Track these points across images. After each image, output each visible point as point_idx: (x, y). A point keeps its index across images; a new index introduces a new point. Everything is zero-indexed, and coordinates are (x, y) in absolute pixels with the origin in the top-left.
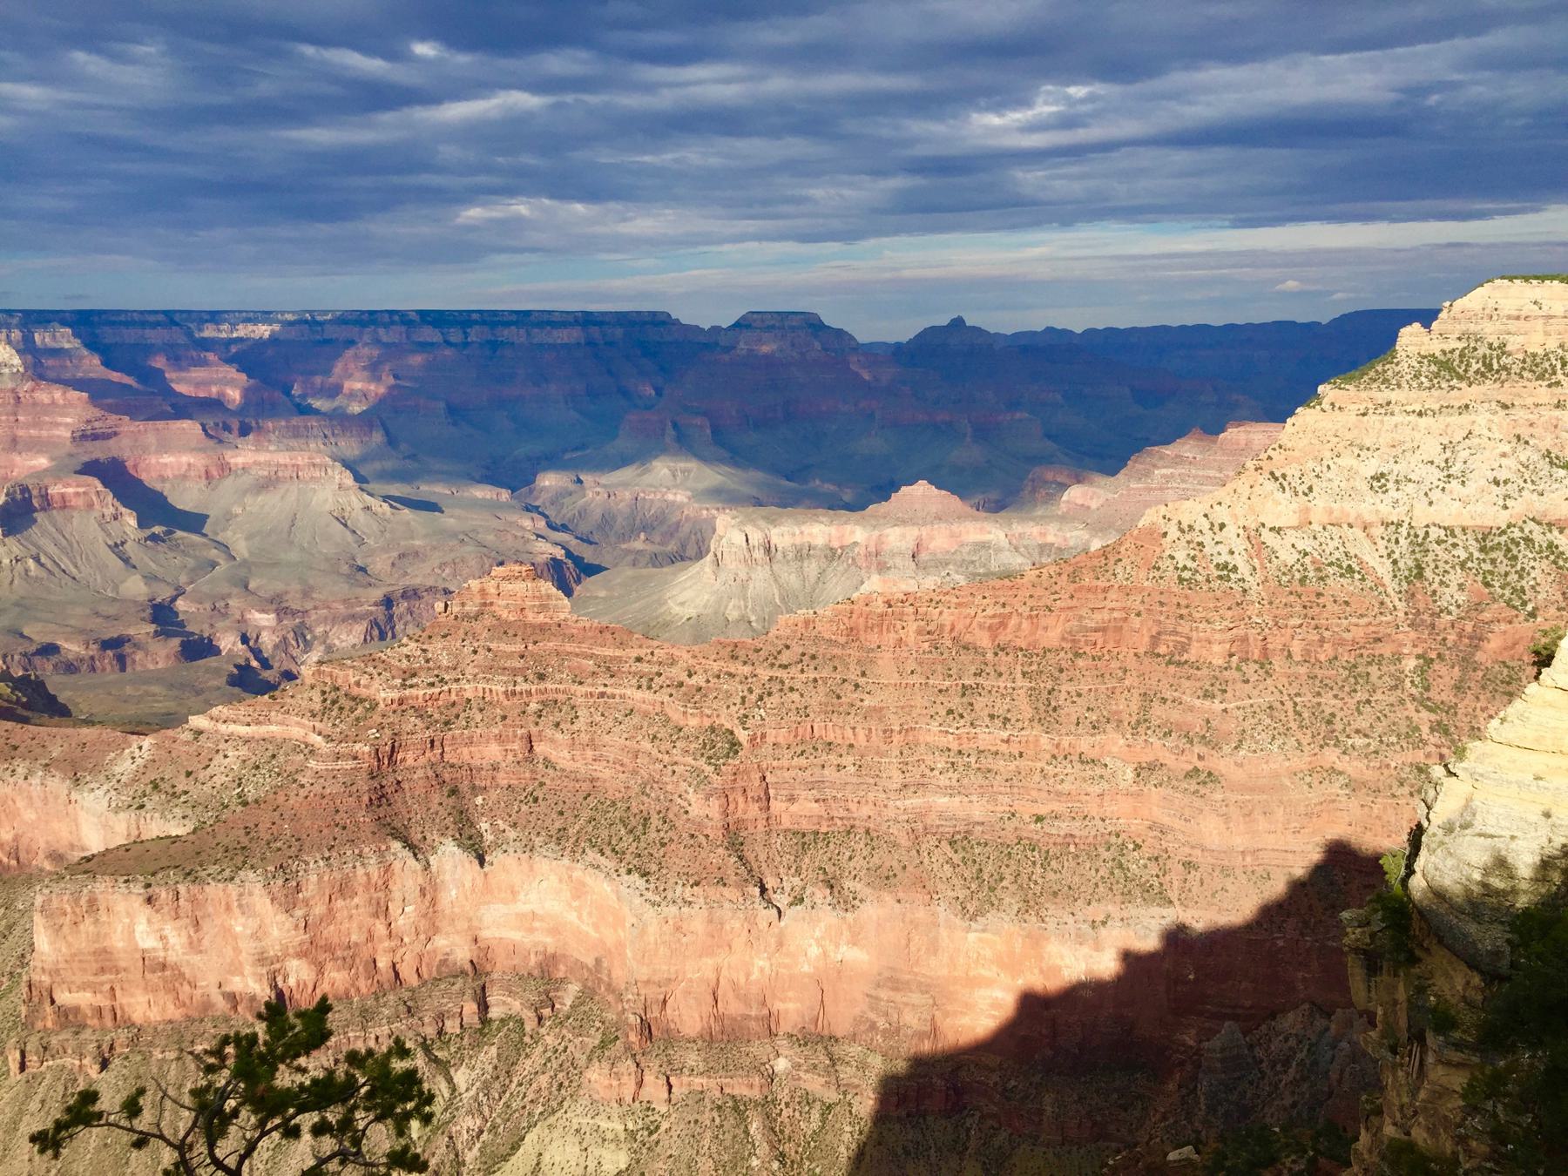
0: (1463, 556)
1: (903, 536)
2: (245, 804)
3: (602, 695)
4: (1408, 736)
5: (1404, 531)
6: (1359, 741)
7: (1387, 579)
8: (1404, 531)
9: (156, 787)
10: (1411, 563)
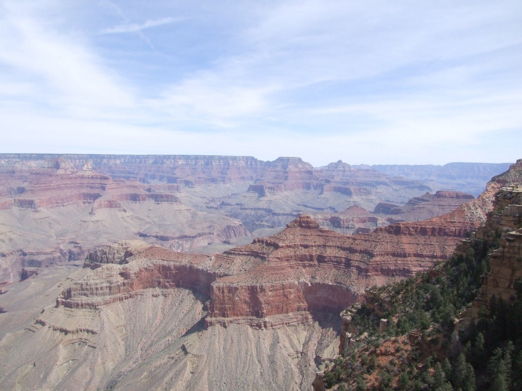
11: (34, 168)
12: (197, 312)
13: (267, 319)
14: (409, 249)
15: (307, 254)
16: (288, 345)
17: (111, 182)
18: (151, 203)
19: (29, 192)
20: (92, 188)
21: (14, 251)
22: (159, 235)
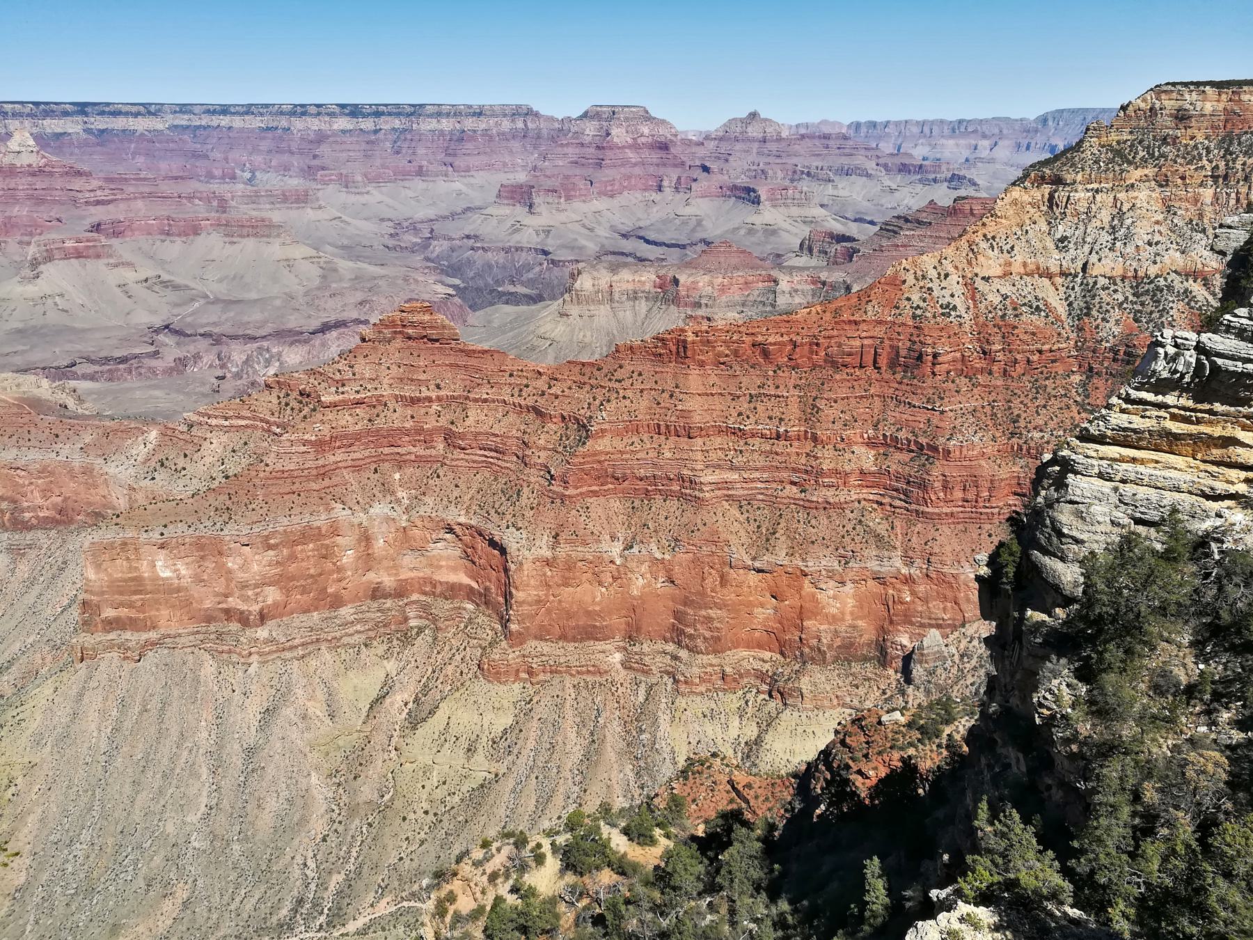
0: (1121, 299)
1: (711, 284)
2: (227, 477)
3: (485, 401)
4: (1071, 430)
5: (1078, 280)
6: (1037, 435)
7: (1064, 317)
8: (1078, 280)
9: (162, 465)
10: (1082, 304)
14: (699, 409)
20: (40, 201)
22: (216, 330)
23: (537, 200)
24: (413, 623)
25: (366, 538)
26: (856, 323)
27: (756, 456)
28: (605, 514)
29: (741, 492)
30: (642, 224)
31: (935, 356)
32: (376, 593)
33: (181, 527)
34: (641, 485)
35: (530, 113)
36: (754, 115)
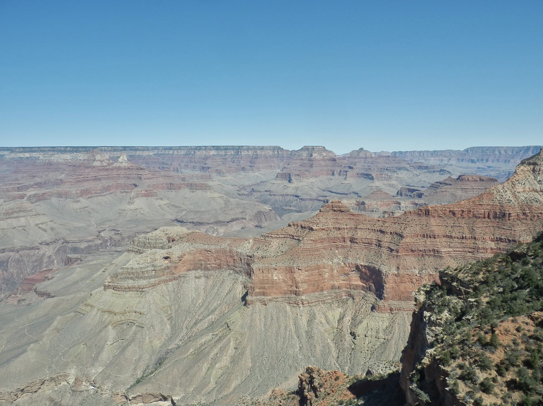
11: (70, 161)
12: (238, 291)
13: (303, 297)
14: (437, 230)
15: (339, 236)
16: (324, 321)
17: (147, 172)
18: (186, 192)
19: (68, 184)
21: (56, 240)
23: (293, 178)
24: (344, 297)
25: (332, 270)
26: (481, 205)
27: (457, 244)
28: (410, 261)
29: (454, 255)
30: (328, 187)
31: (510, 214)
32: (333, 287)
33: (281, 264)
34: (421, 253)
35: (279, 148)
36: (361, 149)
